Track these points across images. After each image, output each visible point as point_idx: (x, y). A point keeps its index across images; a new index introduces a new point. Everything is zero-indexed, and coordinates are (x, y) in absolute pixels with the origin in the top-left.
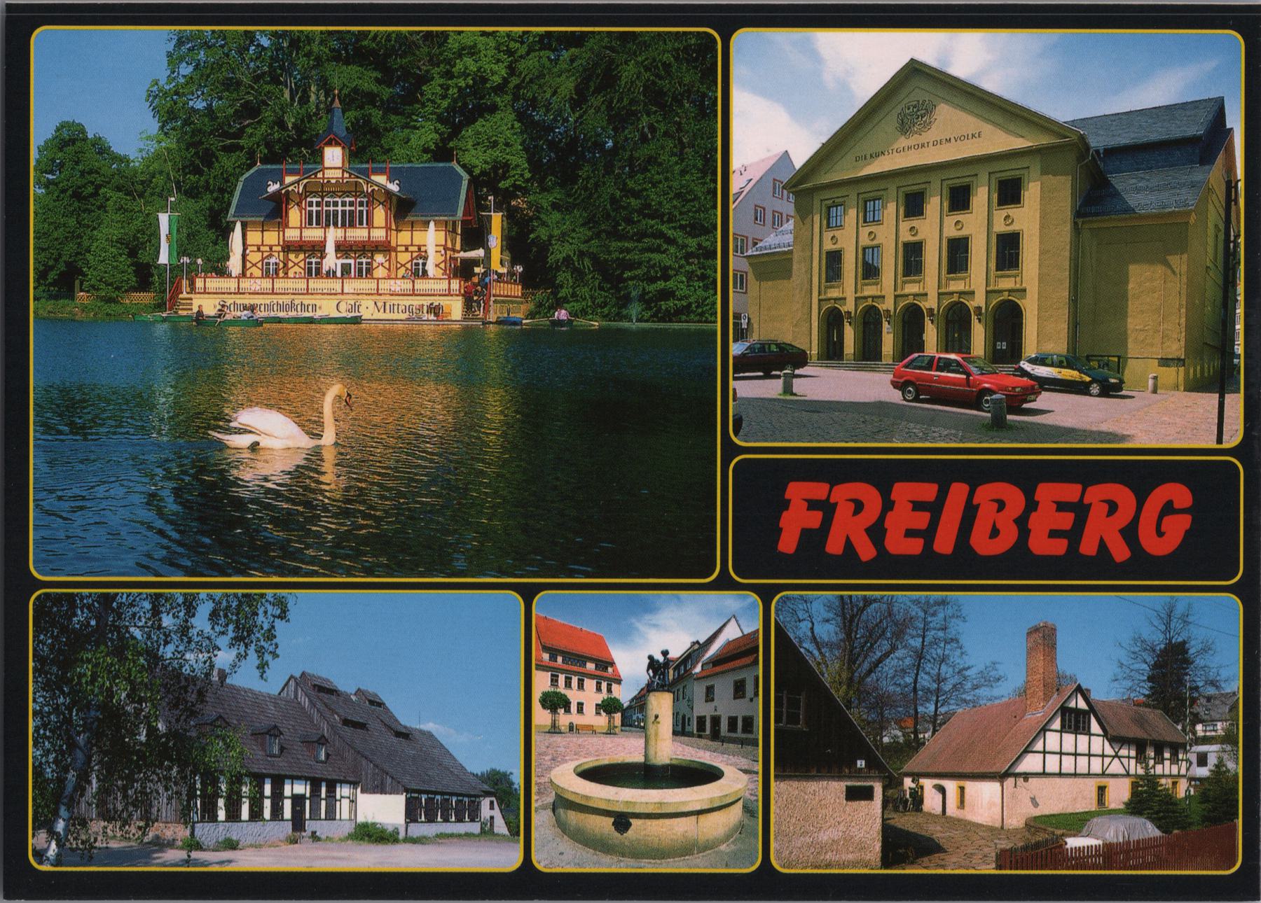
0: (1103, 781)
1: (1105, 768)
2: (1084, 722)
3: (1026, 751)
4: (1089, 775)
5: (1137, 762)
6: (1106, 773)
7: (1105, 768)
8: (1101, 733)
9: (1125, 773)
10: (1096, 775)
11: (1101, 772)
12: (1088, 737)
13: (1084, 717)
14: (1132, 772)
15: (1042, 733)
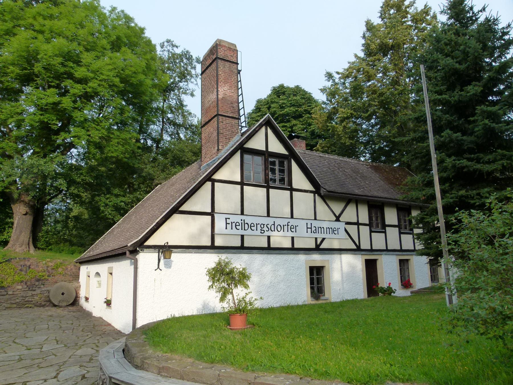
0: (317, 259)
1: (318, 243)
2: (282, 171)
3: (176, 210)
4: (293, 250)
5: (371, 232)
6: (321, 247)
7: (318, 243)
8: (311, 188)
9: (355, 247)
10: (307, 250)
11: (313, 246)
12: (288, 192)
13: (281, 164)
14: (365, 245)
15: (209, 184)
